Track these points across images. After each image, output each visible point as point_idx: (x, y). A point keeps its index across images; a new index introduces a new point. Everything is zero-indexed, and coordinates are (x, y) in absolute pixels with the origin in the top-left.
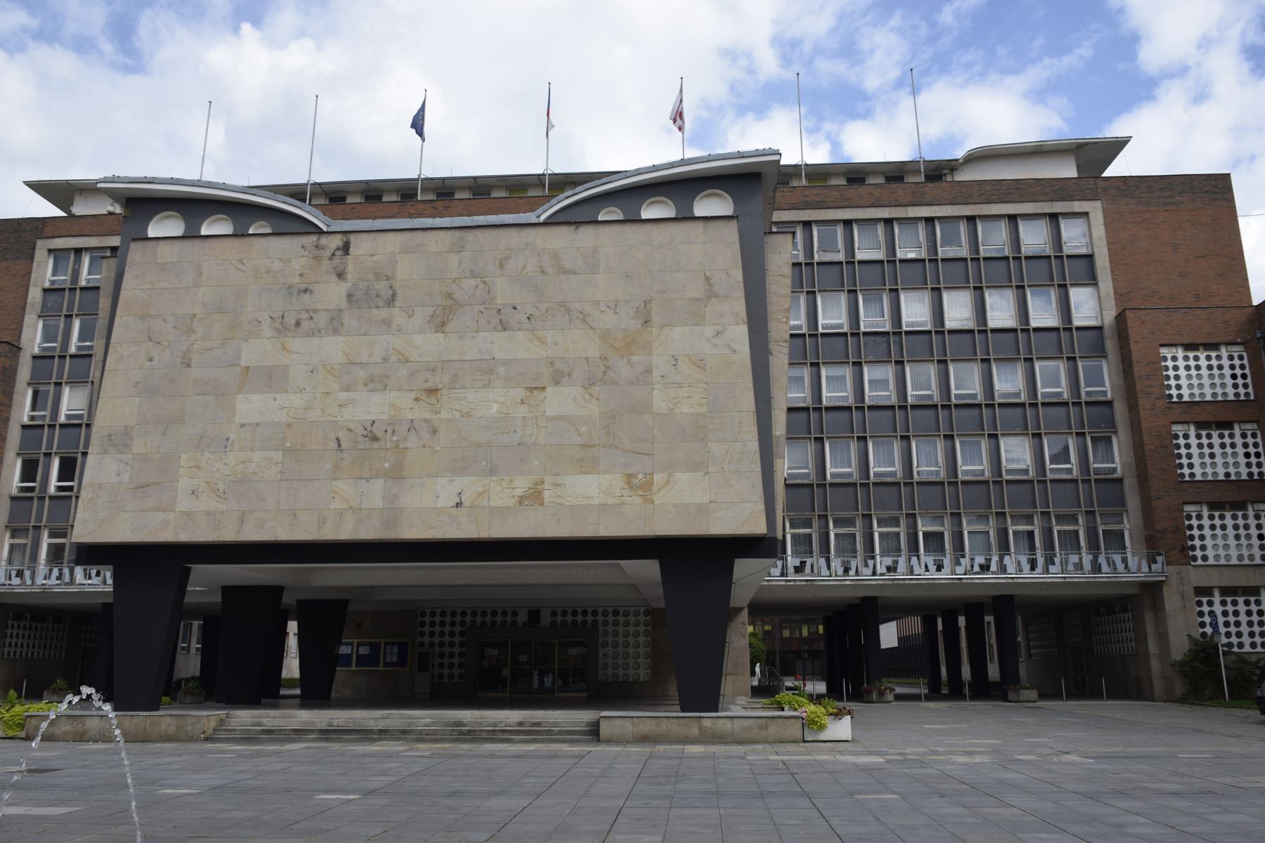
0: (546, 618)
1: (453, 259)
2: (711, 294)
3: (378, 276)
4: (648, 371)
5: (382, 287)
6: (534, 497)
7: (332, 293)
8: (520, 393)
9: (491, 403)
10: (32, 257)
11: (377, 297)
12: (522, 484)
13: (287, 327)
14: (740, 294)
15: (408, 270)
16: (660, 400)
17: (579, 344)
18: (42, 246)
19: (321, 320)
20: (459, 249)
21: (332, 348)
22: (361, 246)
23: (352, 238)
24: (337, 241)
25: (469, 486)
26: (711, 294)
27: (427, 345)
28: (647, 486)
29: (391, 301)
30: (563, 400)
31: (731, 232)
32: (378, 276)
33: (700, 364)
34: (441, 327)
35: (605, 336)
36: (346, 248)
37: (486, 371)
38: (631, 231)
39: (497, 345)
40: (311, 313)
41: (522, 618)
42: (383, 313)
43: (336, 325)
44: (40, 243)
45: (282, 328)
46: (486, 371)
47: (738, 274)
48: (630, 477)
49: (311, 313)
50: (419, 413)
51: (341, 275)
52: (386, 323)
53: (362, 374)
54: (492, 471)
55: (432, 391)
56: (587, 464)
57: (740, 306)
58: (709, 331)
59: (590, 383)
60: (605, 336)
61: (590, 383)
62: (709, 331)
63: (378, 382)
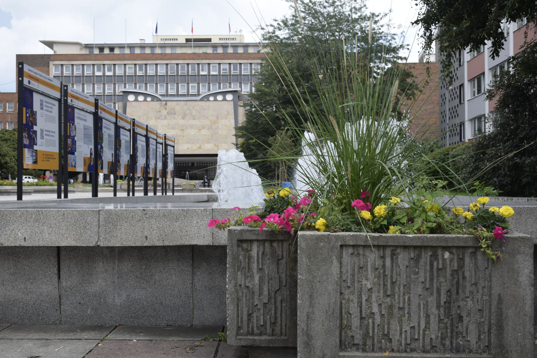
0: (196, 165)
1: (185, 106)
2: (228, 114)
3: (172, 109)
4: (218, 127)
5: (173, 111)
6: (200, 147)
7: (164, 112)
8: (197, 130)
9: (193, 132)
10: (49, 66)
11: (172, 113)
12: (198, 146)
13: (158, 118)
14: (233, 114)
15: (178, 108)
16: (220, 132)
17: (207, 122)
18: (51, 63)
19: (163, 117)
20: (186, 105)
21: (165, 122)
22: (169, 103)
23: (168, 102)
24: (164, 103)
25: (189, 146)
26: (228, 114)
27: (181, 122)
28: (218, 146)
29: (175, 114)
30: (204, 132)
31: (232, 103)
32: (172, 109)
33: (227, 127)
34: (184, 119)
35: (211, 121)
36: (166, 104)
37: (191, 127)
38: (215, 103)
39: (193, 122)
40: (161, 116)
41: (190, 164)
42: (174, 116)
43: (165, 118)
44: (51, 63)
45: (156, 119)
46: (191, 127)
47: (233, 111)
48: (215, 145)
49: (161, 116)
50: (181, 133)
51: (166, 109)
52: (174, 118)
53: (171, 127)
54: (193, 143)
55: (183, 130)
56: (208, 142)
57: (233, 116)
58: (228, 120)
59: (209, 129)
60: (211, 121)
61: (209, 129)
62: (228, 120)
63: (173, 128)
